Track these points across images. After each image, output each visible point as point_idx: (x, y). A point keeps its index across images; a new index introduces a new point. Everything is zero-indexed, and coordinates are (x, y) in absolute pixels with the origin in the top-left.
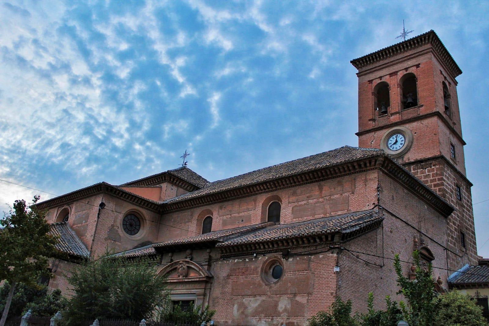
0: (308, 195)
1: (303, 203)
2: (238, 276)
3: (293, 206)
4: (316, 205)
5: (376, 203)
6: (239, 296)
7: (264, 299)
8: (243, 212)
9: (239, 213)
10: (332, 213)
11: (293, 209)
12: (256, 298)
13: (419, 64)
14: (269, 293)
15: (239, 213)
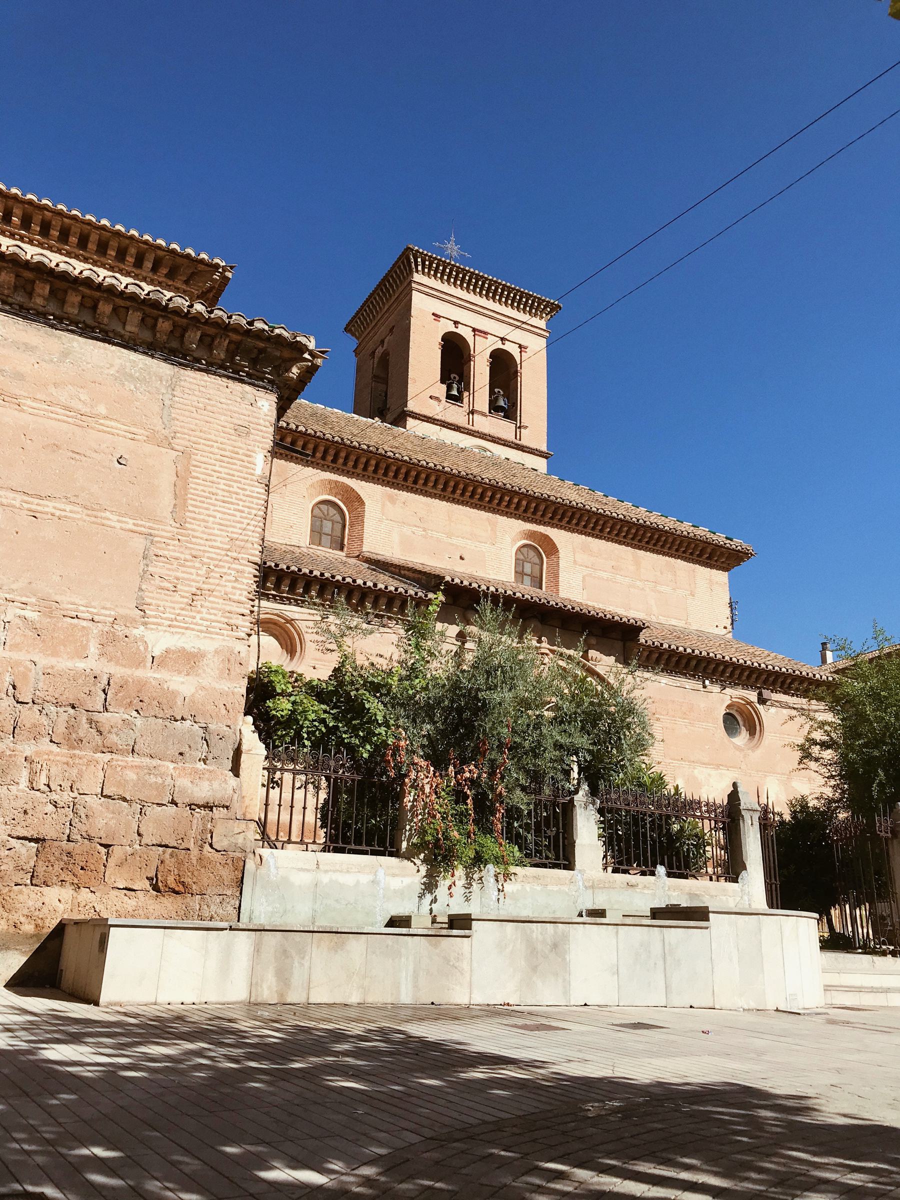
0: (613, 563)
1: (605, 575)
2: (674, 717)
3: (585, 574)
4: (632, 590)
5: (730, 627)
6: (685, 761)
7: (737, 776)
8: (463, 538)
9: (449, 535)
10: (660, 617)
11: (584, 577)
12: (720, 771)
13: (526, 348)
14: (743, 767)
15: (449, 535)
